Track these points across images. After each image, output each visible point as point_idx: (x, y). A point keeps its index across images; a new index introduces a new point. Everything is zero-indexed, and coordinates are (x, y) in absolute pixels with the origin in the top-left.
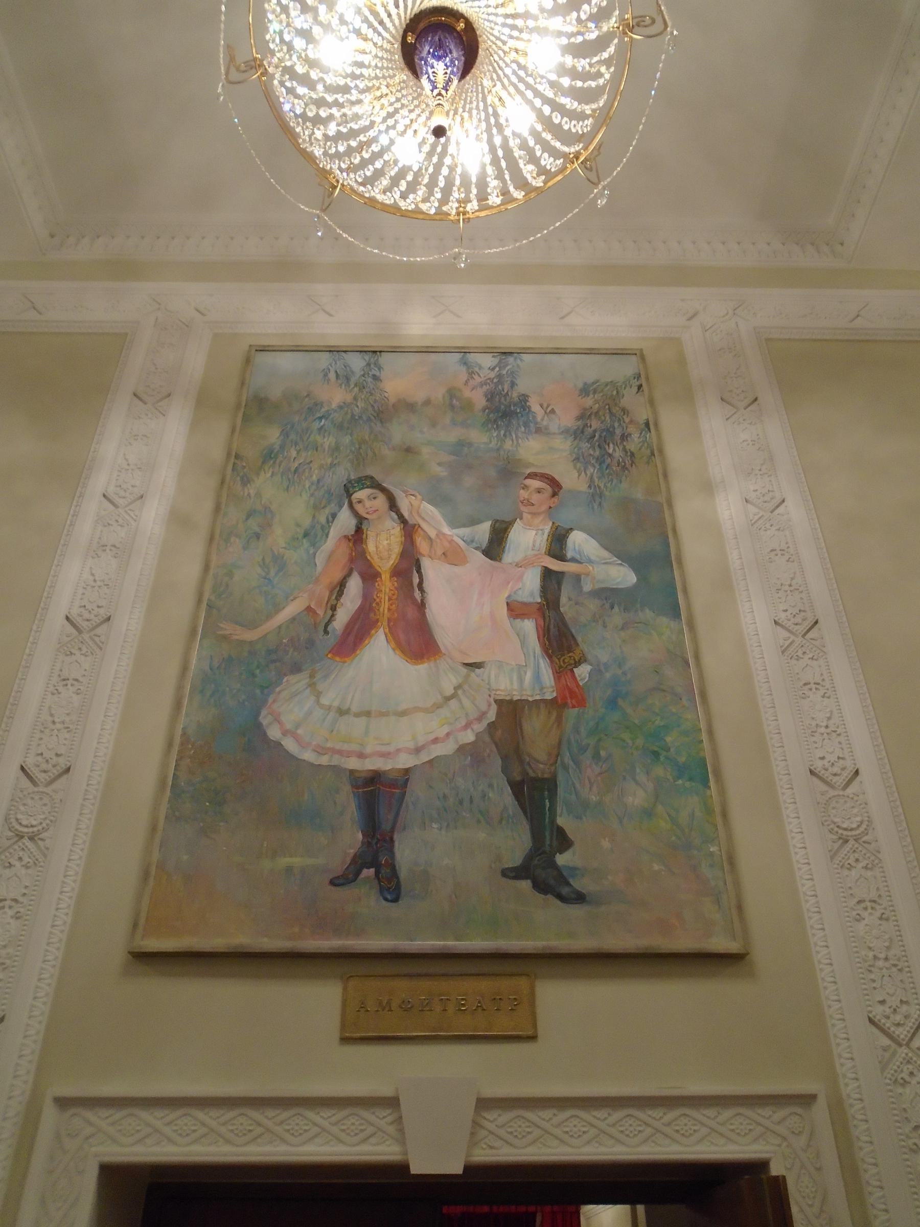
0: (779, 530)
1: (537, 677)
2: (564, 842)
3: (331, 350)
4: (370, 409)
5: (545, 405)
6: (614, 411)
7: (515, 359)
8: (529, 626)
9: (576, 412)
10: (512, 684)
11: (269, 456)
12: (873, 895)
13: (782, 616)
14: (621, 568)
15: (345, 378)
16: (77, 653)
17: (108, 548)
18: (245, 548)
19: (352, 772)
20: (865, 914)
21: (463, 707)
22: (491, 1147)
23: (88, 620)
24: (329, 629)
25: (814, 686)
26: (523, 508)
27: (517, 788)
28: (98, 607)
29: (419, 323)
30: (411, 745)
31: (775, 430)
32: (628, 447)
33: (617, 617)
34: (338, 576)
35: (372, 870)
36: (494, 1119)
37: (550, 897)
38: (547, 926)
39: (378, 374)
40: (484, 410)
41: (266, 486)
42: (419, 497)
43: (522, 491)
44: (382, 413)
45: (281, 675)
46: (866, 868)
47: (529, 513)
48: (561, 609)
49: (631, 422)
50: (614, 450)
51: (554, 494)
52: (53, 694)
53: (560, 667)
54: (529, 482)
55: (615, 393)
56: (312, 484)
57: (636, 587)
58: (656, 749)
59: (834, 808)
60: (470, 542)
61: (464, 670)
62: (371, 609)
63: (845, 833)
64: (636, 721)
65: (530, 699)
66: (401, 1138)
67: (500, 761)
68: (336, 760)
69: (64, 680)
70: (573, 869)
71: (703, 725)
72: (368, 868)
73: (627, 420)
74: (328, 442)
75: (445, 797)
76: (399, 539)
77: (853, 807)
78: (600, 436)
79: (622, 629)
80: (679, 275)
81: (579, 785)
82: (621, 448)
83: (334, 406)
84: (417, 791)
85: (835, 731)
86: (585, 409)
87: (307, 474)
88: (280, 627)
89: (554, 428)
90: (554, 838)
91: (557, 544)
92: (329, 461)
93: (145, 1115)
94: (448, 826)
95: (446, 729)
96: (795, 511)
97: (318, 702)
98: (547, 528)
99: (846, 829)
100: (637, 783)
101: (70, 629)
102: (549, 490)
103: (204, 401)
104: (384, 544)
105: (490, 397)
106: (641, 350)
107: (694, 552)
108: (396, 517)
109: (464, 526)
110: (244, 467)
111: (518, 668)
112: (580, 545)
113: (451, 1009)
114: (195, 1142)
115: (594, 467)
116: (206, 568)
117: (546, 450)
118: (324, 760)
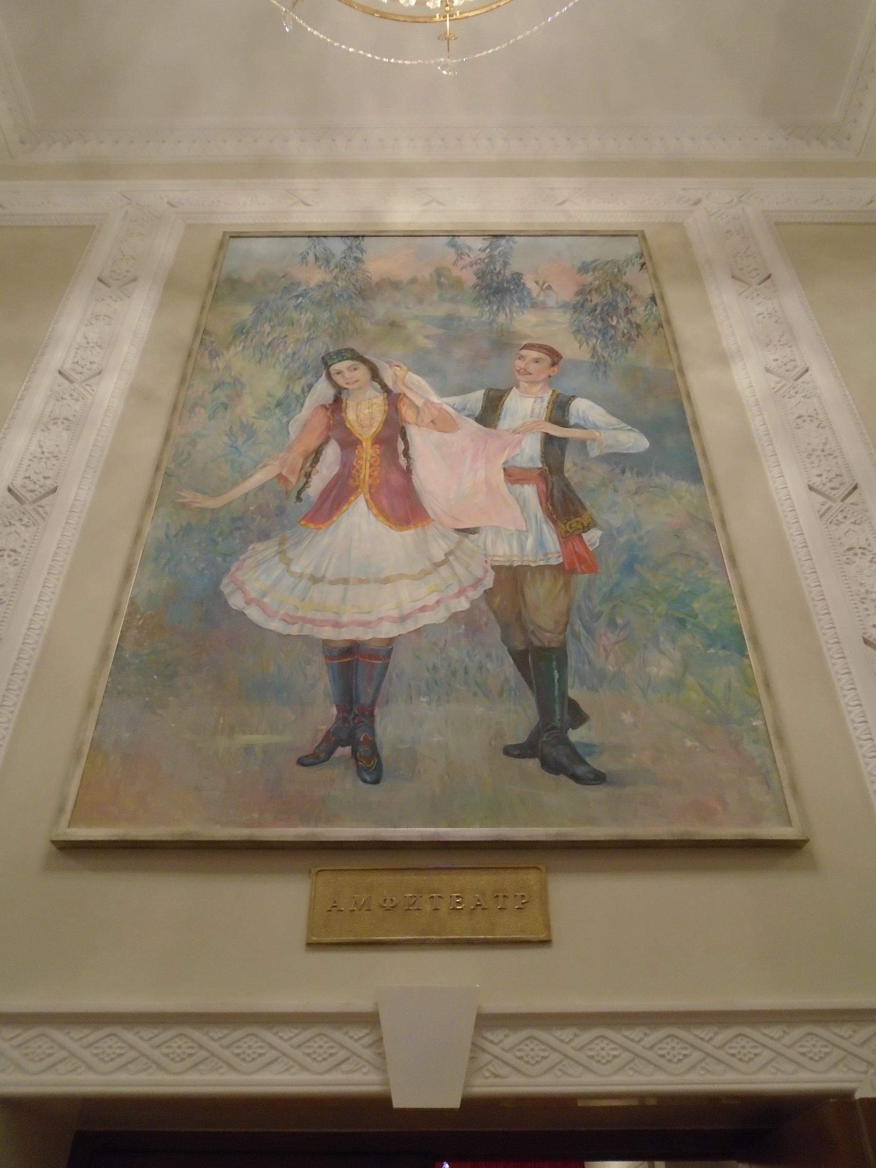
0: (805, 397)
1: (540, 542)
2: (577, 716)
3: (309, 236)
4: (351, 287)
5: (541, 283)
6: (616, 287)
7: (507, 241)
8: (530, 492)
9: (574, 288)
10: (511, 549)
11: (241, 331)
13: (816, 481)
14: (632, 434)
15: (325, 260)
16: (18, 524)
17: (59, 422)
18: (210, 418)
19: (326, 642)
21: (455, 574)
22: (496, 1076)
23: (32, 491)
24: (303, 496)
25: (859, 551)
26: (519, 377)
27: (520, 658)
29: (404, 211)
30: (395, 613)
31: (793, 304)
32: (632, 320)
33: (630, 481)
34: (313, 443)
35: (348, 749)
36: (500, 1041)
37: (562, 777)
38: (559, 811)
39: (360, 256)
40: (475, 287)
41: (237, 360)
42: (405, 368)
43: (518, 361)
44: (365, 291)
45: (246, 542)
47: (527, 382)
48: (566, 475)
49: (635, 296)
50: (618, 322)
51: (554, 364)
53: (567, 532)
54: (524, 352)
55: (616, 270)
56: (287, 356)
57: (648, 451)
58: (681, 616)
60: (461, 410)
61: (456, 536)
62: (349, 475)
64: (657, 587)
65: (533, 565)
66: (382, 1066)
67: (499, 630)
68: (307, 630)
70: (590, 746)
71: (735, 590)
72: (343, 746)
73: (631, 295)
74: (305, 318)
75: (435, 668)
76: (382, 408)
78: (602, 309)
79: (636, 493)
80: (676, 167)
81: (593, 657)
82: (625, 320)
83: (312, 284)
84: (401, 661)
86: (584, 285)
87: (281, 347)
88: (247, 494)
89: (551, 302)
90: (566, 712)
91: (559, 412)
92: (306, 335)
93: (58, 1035)
94: (439, 699)
95: (435, 597)
96: (823, 379)
97: (288, 569)
98: (547, 396)
100: (662, 652)
101: (11, 500)
102: (548, 360)
103: (172, 285)
104: (365, 413)
105: (481, 275)
106: (643, 232)
107: (712, 423)
108: (379, 386)
109: (455, 394)
110: (212, 342)
111: (520, 533)
112: (584, 412)
113: (444, 908)
114: (119, 1069)
115: (597, 338)
116: (167, 436)
117: (545, 322)
118: (294, 630)
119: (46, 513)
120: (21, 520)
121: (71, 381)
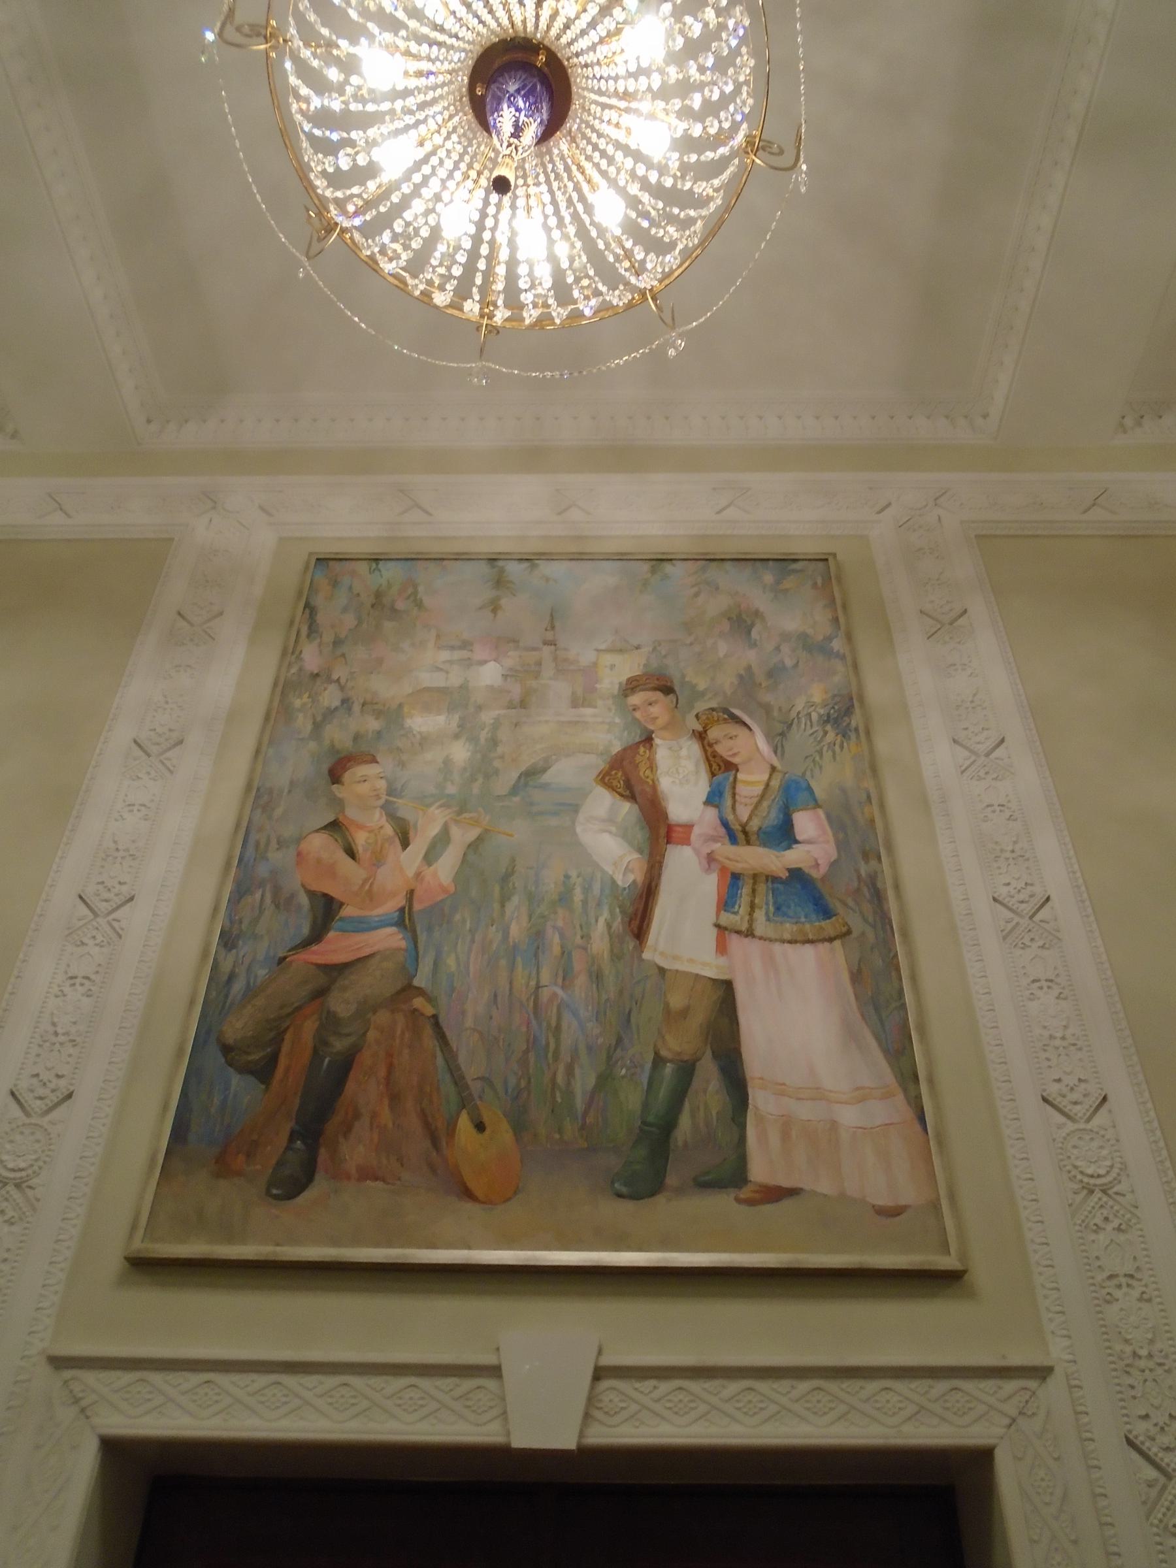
12: (1129, 1268)
13: (1003, 892)
16: (91, 942)
20: (1118, 1294)
23: (106, 901)
25: (1045, 984)
28: (120, 883)
46: (1119, 1229)
52: (57, 996)
59: (1075, 1147)
63: (1092, 1181)
69: (71, 978)
77: (1101, 1147)
85: (1074, 1045)
99: (1092, 1176)
121: (149, 755)
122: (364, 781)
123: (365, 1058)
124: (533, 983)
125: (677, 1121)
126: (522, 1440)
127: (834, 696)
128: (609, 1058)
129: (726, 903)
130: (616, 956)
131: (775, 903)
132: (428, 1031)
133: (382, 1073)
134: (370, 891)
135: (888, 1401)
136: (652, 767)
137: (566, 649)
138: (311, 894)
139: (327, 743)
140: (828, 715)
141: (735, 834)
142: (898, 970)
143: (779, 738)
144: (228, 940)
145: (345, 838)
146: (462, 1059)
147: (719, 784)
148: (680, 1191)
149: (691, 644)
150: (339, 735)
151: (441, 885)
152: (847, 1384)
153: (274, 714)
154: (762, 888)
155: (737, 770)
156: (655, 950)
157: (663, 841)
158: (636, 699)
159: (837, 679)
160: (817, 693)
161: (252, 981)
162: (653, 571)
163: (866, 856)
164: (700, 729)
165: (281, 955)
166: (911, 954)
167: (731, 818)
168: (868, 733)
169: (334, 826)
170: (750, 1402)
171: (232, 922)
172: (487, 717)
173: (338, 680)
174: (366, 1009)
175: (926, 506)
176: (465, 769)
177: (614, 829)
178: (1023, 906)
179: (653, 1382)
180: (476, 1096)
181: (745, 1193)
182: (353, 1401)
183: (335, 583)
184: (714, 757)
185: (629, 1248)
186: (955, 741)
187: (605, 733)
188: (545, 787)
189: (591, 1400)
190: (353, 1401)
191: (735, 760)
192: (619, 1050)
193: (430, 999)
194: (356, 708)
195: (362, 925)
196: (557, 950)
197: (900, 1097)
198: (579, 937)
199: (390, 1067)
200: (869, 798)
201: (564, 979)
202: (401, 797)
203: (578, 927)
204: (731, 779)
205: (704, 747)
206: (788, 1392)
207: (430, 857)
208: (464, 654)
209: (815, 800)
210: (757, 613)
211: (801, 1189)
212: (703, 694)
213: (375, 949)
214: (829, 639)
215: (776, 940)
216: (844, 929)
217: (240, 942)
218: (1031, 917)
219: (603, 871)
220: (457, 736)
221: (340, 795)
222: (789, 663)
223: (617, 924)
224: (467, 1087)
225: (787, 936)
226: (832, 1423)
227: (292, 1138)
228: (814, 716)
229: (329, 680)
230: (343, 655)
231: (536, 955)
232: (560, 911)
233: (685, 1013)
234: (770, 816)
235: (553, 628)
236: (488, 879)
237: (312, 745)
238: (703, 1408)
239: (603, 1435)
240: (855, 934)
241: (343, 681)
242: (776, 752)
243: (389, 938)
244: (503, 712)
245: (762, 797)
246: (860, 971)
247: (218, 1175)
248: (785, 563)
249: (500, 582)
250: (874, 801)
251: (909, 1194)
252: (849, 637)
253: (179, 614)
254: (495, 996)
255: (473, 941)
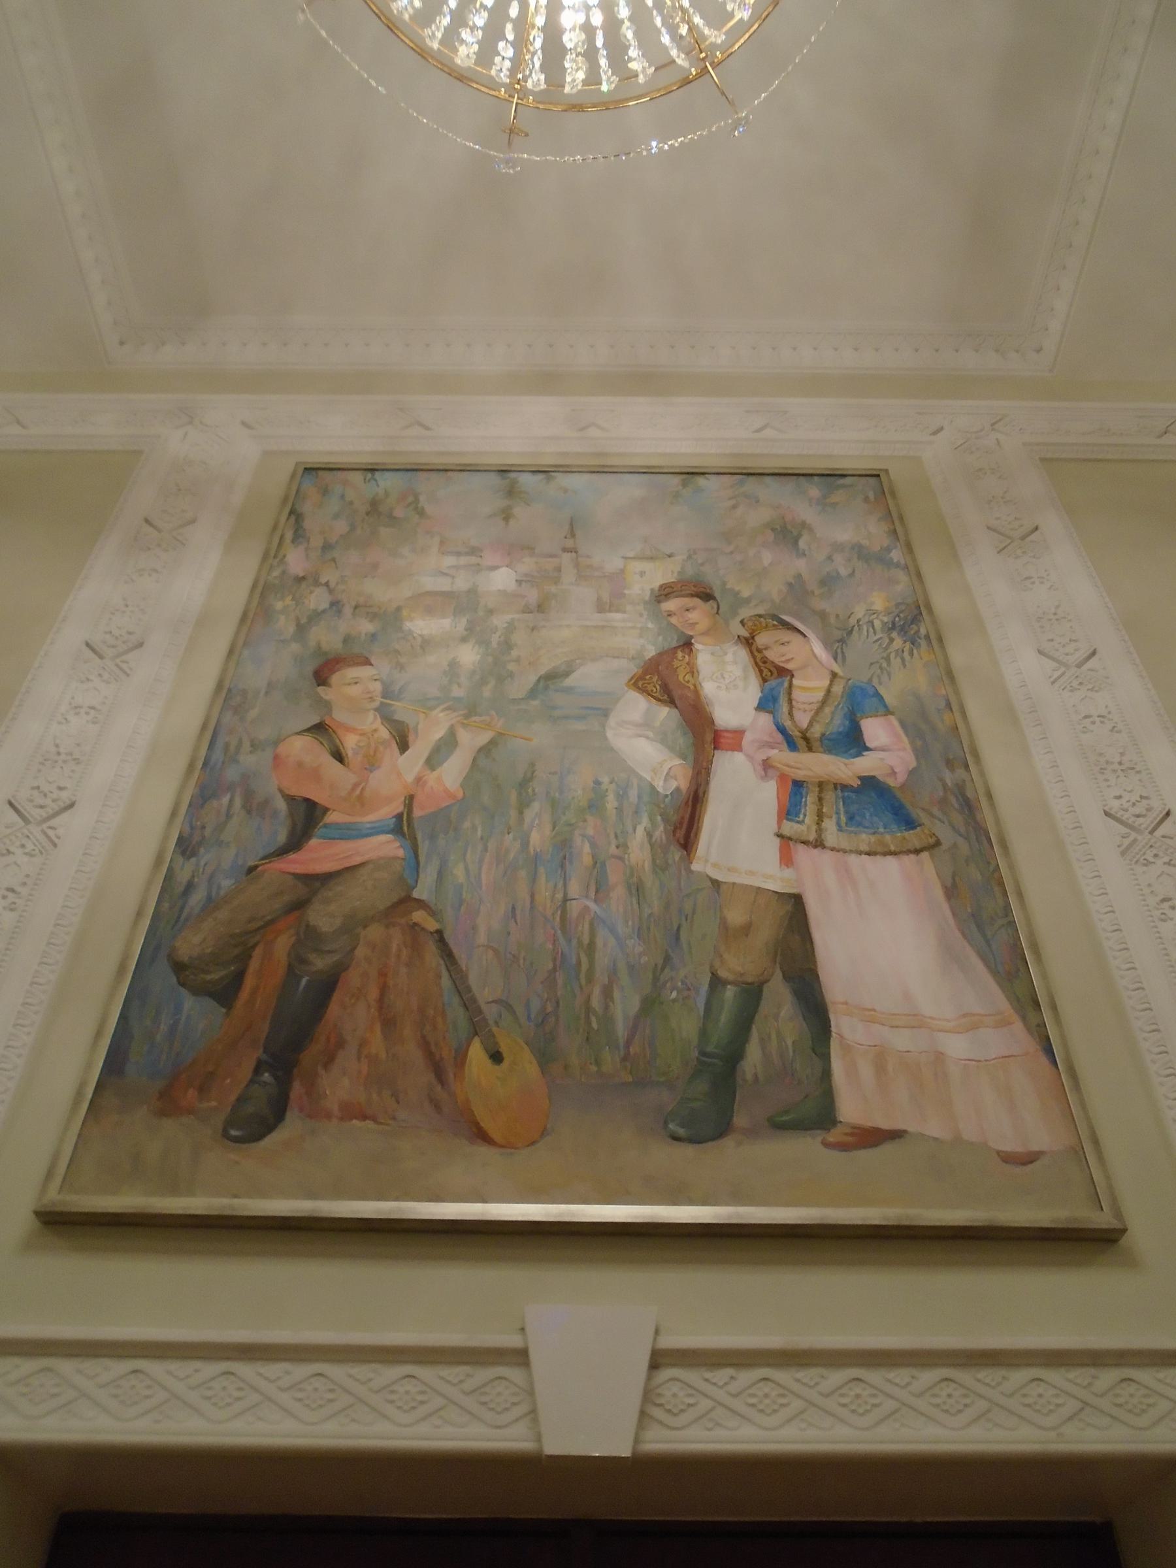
13: (1116, 804)
16: (19, 852)
23: (42, 807)
119: (59, 838)
120: (23, 846)
121: (101, 657)
122: (354, 686)
123: (353, 978)
124: (559, 896)
125: (743, 1047)
126: (556, 1445)
127: (898, 605)
128: (656, 979)
129: (789, 810)
130: (660, 867)
131: (846, 812)
132: (431, 948)
133: (373, 994)
134: (360, 797)
135: (1040, 1396)
136: (693, 671)
137: (588, 557)
138: (290, 799)
139: (312, 643)
140: (893, 623)
141: (793, 740)
142: (1001, 884)
143: (838, 644)
144: (186, 847)
145: (331, 741)
146: (473, 980)
147: (772, 689)
148: (752, 1133)
149: (732, 553)
150: (327, 637)
151: (446, 791)
152: (984, 1374)
153: (251, 615)
154: (830, 796)
155: (793, 676)
156: (707, 861)
157: (709, 747)
158: (671, 605)
159: (899, 588)
160: (879, 602)
161: (214, 894)
162: (684, 485)
163: (949, 764)
164: (747, 634)
165: (251, 863)
166: (1011, 867)
167: (788, 724)
168: (940, 640)
169: (320, 729)
170: (858, 1396)
171: (192, 828)
172: (499, 621)
173: (327, 584)
174: (352, 925)
175: (981, 430)
176: (474, 672)
177: (651, 734)
178: (1141, 820)
179: (730, 1371)
180: (491, 1022)
181: (834, 1136)
182: (331, 1396)
183: (325, 492)
184: (765, 662)
185: (691, 1202)
186: (1040, 652)
187: (637, 637)
188: (569, 690)
189: (649, 1396)
190: (331, 1396)
191: (789, 666)
192: (667, 970)
193: (433, 913)
194: (347, 610)
195: (350, 833)
196: (587, 860)
197: (1018, 1026)
198: (613, 847)
199: (384, 989)
200: (949, 706)
201: (597, 892)
202: (399, 700)
203: (612, 836)
204: (786, 684)
205: (752, 652)
206: (908, 1384)
207: (432, 762)
208: (473, 560)
209: (885, 706)
210: (804, 525)
211: (905, 1131)
212: (747, 601)
213: (366, 858)
214: (888, 550)
215: (851, 851)
216: (932, 841)
217: (202, 850)
218: (1151, 832)
219: (641, 778)
220: (464, 640)
221: (327, 698)
222: (844, 572)
223: (660, 833)
224: (480, 1012)
225: (864, 847)
226: (969, 1425)
227: (257, 1070)
228: (877, 623)
229: (317, 583)
230: (334, 560)
231: (562, 866)
232: (590, 818)
233: (746, 929)
234: (833, 721)
235: (573, 535)
236: (501, 785)
237: (295, 647)
238: (797, 1404)
239: (659, 1442)
240: (944, 847)
241: (332, 585)
242: (835, 659)
243: (385, 846)
244: (516, 616)
245: (824, 703)
246: (954, 884)
247: (162, 1113)
248: (833, 479)
249: (512, 492)
250: (955, 708)
251: (1041, 1134)
252: (909, 547)
253: (147, 521)
254: (514, 908)
255: (486, 849)
